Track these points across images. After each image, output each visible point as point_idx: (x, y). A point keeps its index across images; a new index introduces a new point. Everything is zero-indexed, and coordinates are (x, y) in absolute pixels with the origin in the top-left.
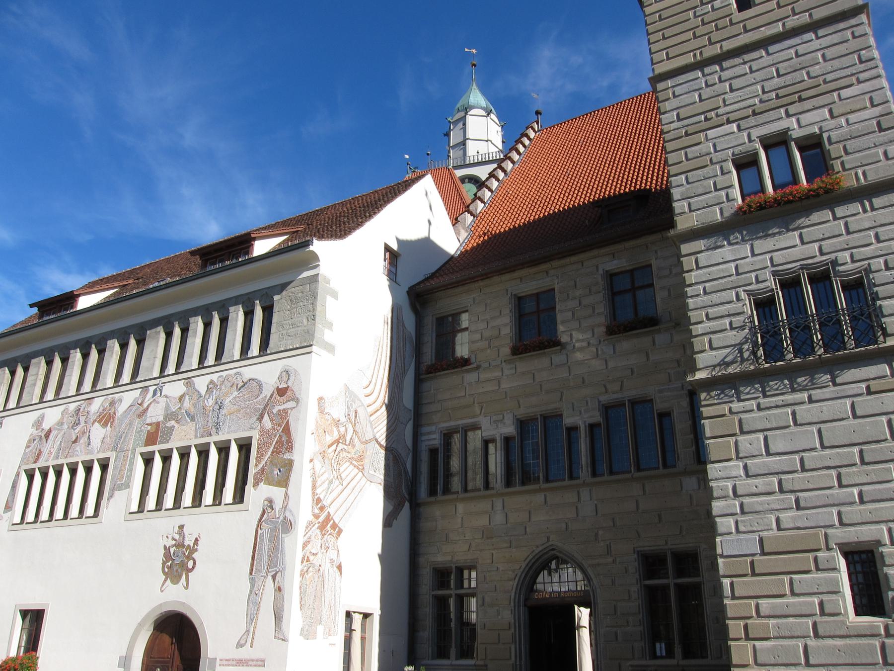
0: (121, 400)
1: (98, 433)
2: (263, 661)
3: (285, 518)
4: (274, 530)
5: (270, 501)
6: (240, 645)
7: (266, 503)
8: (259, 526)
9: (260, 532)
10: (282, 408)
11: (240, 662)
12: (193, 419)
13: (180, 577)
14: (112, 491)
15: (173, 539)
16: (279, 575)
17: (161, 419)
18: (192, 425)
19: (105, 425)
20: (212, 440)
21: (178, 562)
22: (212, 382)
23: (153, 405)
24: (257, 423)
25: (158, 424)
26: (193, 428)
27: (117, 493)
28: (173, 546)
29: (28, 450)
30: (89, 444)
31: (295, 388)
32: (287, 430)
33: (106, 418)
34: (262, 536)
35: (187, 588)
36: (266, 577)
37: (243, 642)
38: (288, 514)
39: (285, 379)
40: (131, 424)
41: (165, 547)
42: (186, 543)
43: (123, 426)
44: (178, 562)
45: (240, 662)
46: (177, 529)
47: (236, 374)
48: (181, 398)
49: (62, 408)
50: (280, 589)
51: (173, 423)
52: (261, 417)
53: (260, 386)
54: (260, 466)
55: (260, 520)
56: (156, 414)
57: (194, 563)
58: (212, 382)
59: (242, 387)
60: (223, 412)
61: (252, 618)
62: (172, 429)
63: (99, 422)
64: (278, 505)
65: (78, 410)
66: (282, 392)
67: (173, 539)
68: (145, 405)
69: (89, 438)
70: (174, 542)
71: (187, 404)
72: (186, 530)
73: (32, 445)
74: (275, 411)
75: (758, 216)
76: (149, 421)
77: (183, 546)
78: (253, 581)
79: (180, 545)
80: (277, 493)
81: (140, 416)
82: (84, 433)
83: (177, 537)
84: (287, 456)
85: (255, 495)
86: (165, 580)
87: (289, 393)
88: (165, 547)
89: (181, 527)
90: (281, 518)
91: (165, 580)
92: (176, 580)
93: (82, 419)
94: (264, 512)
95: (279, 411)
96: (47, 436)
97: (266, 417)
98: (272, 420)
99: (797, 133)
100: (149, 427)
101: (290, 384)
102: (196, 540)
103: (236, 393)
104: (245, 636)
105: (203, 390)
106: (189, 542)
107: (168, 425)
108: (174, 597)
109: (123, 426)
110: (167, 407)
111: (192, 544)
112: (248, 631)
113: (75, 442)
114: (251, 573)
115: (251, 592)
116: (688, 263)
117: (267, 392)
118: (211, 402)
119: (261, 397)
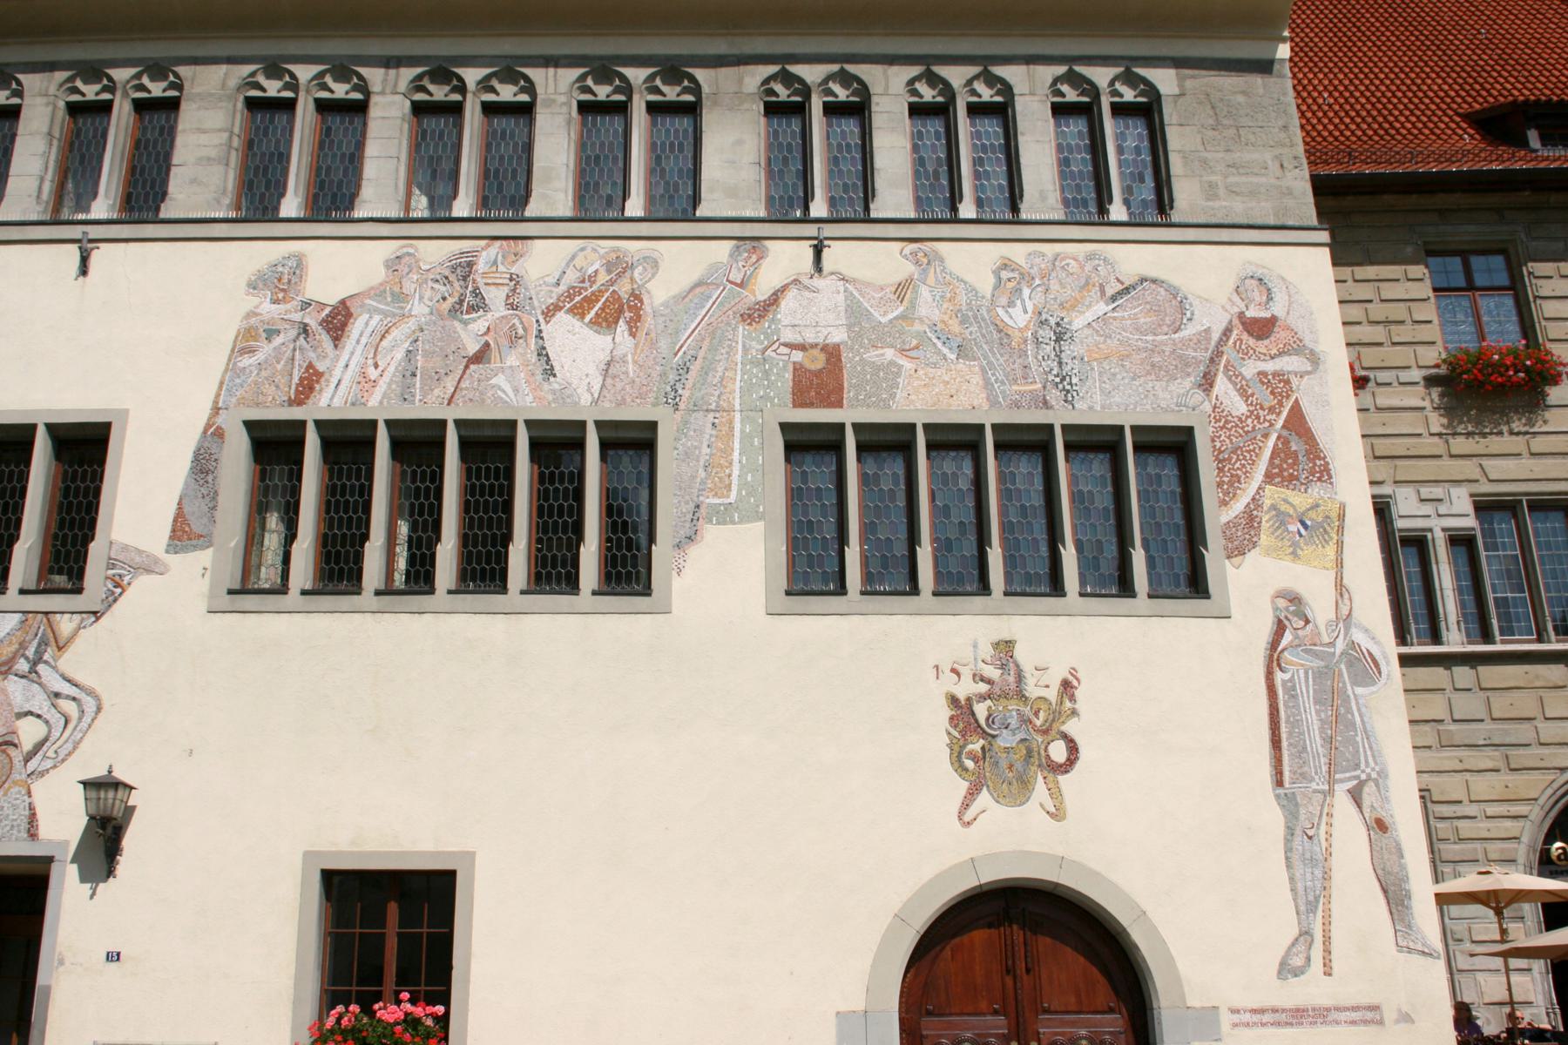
0: (653, 264)
2: (1374, 1008)
3: (1353, 645)
4: (1325, 676)
5: (1295, 599)
6: (1287, 970)
7: (1282, 603)
8: (1273, 661)
9: (1279, 677)
10: (1270, 367)
11: (1298, 1016)
12: (962, 351)
13: (1025, 785)
16: (1369, 789)
17: (838, 336)
19: (606, 321)
21: (1006, 739)
22: (1006, 265)
23: (792, 293)
24: (1199, 395)
25: (833, 353)
26: (977, 379)
27: (712, 533)
28: (982, 698)
29: (246, 361)
30: (550, 372)
31: (1293, 321)
33: (612, 308)
35: (1057, 815)
36: (1331, 792)
37: (1298, 961)
38: (1358, 636)
39: (1259, 296)
41: (953, 701)
42: (1032, 691)
44: (1006, 739)
45: (1298, 1016)
46: (987, 651)
47: (1090, 257)
48: (902, 289)
49: (389, 248)
50: (1382, 825)
51: (889, 354)
52: (1207, 383)
53: (1181, 304)
54: (1238, 506)
55: (1274, 644)
56: (815, 316)
57: (1073, 748)
58: (1006, 265)
59: (1120, 294)
60: (1069, 350)
61: (1312, 899)
62: (892, 370)
63: (579, 311)
64: (1322, 608)
65: (464, 269)
66: (1261, 328)
69: (542, 353)
70: (983, 688)
72: (1020, 653)
73: (265, 350)
74: (1250, 369)
76: (789, 336)
77: (1021, 696)
78: (1290, 805)
82: (514, 339)
83: (993, 673)
84: (1316, 491)
85: (1247, 580)
86: (973, 793)
87: (1279, 335)
88: (953, 701)
89: (1005, 648)
90: (1340, 645)
91: (973, 793)
92: (1017, 789)
93: (496, 297)
94: (1280, 628)
96: (338, 321)
97: (1222, 385)
98: (1244, 394)
100: (798, 356)
101: (1278, 309)
102: (1066, 685)
103: (1102, 308)
104: (1301, 947)
105: (986, 284)
107: (872, 355)
108: (1015, 840)
110: (855, 314)
111: (1052, 694)
112: (1305, 933)
113: (480, 357)
114: (1279, 783)
115: (1290, 831)
118: (1019, 318)
119: (1188, 331)
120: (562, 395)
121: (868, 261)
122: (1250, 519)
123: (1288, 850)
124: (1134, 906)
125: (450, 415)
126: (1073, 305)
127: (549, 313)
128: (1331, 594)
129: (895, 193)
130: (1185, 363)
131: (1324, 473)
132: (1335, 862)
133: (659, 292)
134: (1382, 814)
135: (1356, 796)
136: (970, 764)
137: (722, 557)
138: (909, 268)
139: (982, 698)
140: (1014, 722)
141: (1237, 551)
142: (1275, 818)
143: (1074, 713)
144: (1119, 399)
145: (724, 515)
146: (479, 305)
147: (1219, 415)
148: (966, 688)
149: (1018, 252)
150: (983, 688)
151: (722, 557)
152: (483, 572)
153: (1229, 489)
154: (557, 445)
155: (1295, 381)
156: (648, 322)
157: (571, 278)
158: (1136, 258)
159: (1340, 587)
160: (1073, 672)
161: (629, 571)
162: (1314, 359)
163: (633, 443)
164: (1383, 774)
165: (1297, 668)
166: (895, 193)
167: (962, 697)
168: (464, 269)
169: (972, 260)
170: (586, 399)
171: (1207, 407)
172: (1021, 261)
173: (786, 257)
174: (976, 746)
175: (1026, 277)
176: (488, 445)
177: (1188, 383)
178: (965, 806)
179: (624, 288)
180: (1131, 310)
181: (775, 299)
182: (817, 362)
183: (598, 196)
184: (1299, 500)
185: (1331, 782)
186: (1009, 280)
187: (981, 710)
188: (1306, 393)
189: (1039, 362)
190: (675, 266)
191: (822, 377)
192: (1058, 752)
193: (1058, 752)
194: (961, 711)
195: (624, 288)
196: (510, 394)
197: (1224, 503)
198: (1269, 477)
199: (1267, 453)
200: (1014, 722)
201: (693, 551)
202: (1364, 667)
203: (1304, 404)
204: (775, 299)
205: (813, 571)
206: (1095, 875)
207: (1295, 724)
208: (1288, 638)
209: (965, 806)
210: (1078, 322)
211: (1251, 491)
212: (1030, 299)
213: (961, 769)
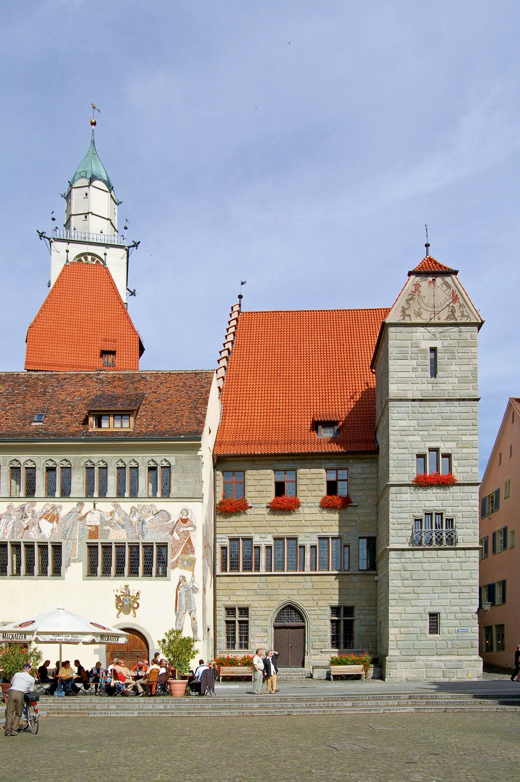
0: (61, 507)
1: (47, 527)
3: (193, 586)
5: (184, 577)
7: (181, 578)
9: (179, 592)
10: (185, 529)
12: (123, 527)
14: (69, 561)
15: (122, 592)
17: (98, 523)
18: (124, 531)
19: (51, 521)
20: (141, 541)
21: (126, 603)
23: (89, 514)
24: (170, 536)
25: (97, 527)
26: (125, 533)
27: (72, 564)
28: (122, 596)
30: (41, 532)
32: (189, 541)
33: (52, 517)
34: (180, 594)
35: (135, 616)
38: (195, 584)
39: (185, 514)
40: (73, 524)
41: (116, 596)
42: (131, 594)
43: (68, 524)
44: (126, 603)
46: (123, 587)
47: (151, 505)
48: (112, 513)
49: (7, 504)
51: (108, 527)
52: (172, 533)
53: (169, 515)
54: (175, 559)
55: (178, 586)
56: (93, 519)
57: (138, 605)
59: (156, 514)
60: (144, 526)
62: (109, 531)
63: (46, 518)
64: (188, 579)
65: (23, 508)
66: (185, 521)
67: (122, 592)
68: (83, 513)
69: (39, 527)
70: (122, 594)
71: (116, 517)
72: (129, 587)
74: (181, 530)
75: (422, 483)
76: (88, 524)
77: (130, 596)
78: (177, 615)
79: (127, 594)
80: (188, 574)
81: (80, 520)
82: (34, 524)
83: (124, 591)
84: (191, 556)
85: (175, 574)
86: (119, 613)
87: (189, 522)
88: (116, 596)
89: (127, 586)
90: (191, 586)
91: (119, 613)
92: (127, 612)
93: (29, 515)
94: (180, 583)
95: (184, 531)
97: (175, 533)
98: (179, 535)
99: (442, 451)
100: (90, 528)
101: (189, 517)
102: (138, 593)
103: (152, 517)
106: (133, 594)
107: (104, 528)
109: (68, 524)
110: (102, 518)
111: (135, 595)
113: (27, 528)
115: (177, 619)
116: (391, 497)
117: (175, 519)
118: (135, 519)
119: (170, 522)
120: (43, 537)
121: (105, 506)
122: (177, 561)
123: (176, 623)
124: (147, 632)
125: (22, 540)
126: (146, 517)
127: (40, 518)
128: (191, 576)
129: (112, 491)
130: (168, 529)
131: (193, 552)
132: (184, 625)
133: (63, 514)
134: (194, 617)
135: (190, 614)
136: (119, 607)
137: (75, 569)
138: (113, 508)
139: (122, 596)
140: (128, 600)
141: (173, 568)
142: (175, 617)
143: (139, 598)
144: (153, 537)
145: (75, 561)
146: (26, 517)
147: (174, 540)
148: (119, 594)
149: (136, 505)
150: (122, 594)
151: (75, 569)
152: (30, 571)
153: (173, 555)
154: (43, 547)
155: (190, 532)
156: (60, 521)
157: (45, 510)
158: (161, 505)
159: (193, 575)
160: (139, 591)
161: (57, 572)
162: (195, 528)
163: (57, 548)
164: (196, 610)
165: (182, 590)
166: (112, 491)
167: (118, 595)
168: (23, 508)
169: (126, 506)
170: (48, 537)
171: (171, 538)
172: (136, 507)
173: (88, 506)
174: (121, 604)
175: (137, 510)
176: (30, 547)
177: (168, 533)
178: (118, 615)
179: (55, 513)
180: (158, 517)
181: (86, 515)
182: (94, 529)
183: (50, 493)
184: (187, 557)
185: (186, 611)
186: (134, 511)
187: (122, 598)
188: (192, 535)
189: (138, 529)
190: (66, 507)
191: (94, 533)
192: (135, 605)
193: (135, 605)
194: (118, 598)
195: (55, 513)
196: (33, 536)
197: (172, 558)
198: (182, 553)
199: (182, 548)
200: (128, 600)
201: (69, 568)
202: (195, 590)
203: (192, 538)
204: (86, 515)
205: (92, 571)
206: (141, 627)
207: (180, 600)
208: (181, 584)
209: (118, 615)
210: (147, 520)
211: (178, 556)
212: (138, 515)
213: (117, 608)
